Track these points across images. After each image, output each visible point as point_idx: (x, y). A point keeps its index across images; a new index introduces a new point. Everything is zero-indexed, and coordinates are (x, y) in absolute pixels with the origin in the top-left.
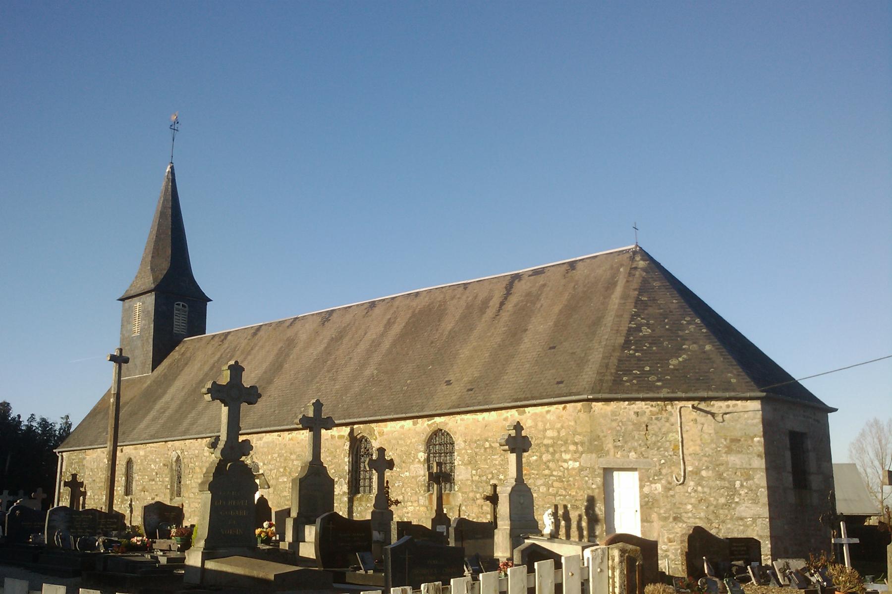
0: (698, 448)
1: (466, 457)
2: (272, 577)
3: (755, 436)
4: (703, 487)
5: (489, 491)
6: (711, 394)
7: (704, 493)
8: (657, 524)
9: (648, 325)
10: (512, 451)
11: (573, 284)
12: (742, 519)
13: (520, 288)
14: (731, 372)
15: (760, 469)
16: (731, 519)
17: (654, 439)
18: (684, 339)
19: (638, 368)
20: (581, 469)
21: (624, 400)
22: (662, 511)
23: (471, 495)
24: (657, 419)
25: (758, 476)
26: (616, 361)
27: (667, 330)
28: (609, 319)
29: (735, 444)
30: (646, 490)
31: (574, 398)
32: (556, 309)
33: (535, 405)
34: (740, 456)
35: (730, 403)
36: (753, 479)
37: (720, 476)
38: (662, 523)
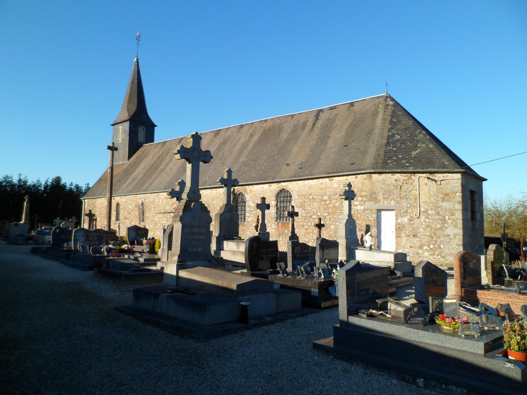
0: (427, 199)
1: (299, 204)
2: (234, 287)
3: (457, 192)
4: (429, 219)
5: (317, 221)
6: (436, 170)
7: (429, 222)
8: (404, 239)
9: (398, 134)
10: (346, 199)
11: (353, 114)
12: (448, 236)
13: (323, 116)
14: (444, 159)
15: (459, 210)
16: (443, 236)
17: (404, 194)
18: (418, 141)
19: (395, 156)
20: (365, 210)
21: (389, 173)
22: (407, 232)
23: (301, 223)
24: (406, 183)
25: (458, 213)
26: (383, 153)
27: (409, 136)
28: (377, 131)
29: (446, 197)
30: (399, 221)
31: (363, 172)
32: (346, 126)
33: (339, 176)
34: (449, 203)
35: (445, 175)
36: (455, 215)
37: (438, 214)
38: (407, 238)
